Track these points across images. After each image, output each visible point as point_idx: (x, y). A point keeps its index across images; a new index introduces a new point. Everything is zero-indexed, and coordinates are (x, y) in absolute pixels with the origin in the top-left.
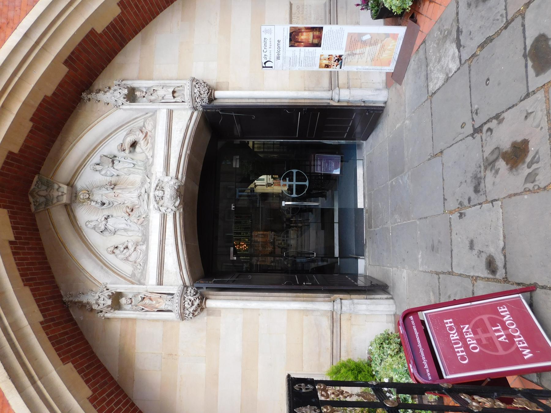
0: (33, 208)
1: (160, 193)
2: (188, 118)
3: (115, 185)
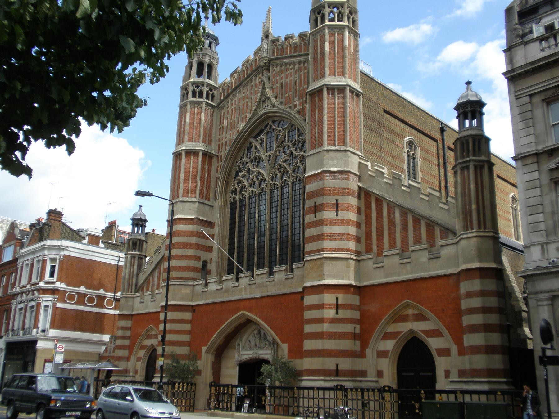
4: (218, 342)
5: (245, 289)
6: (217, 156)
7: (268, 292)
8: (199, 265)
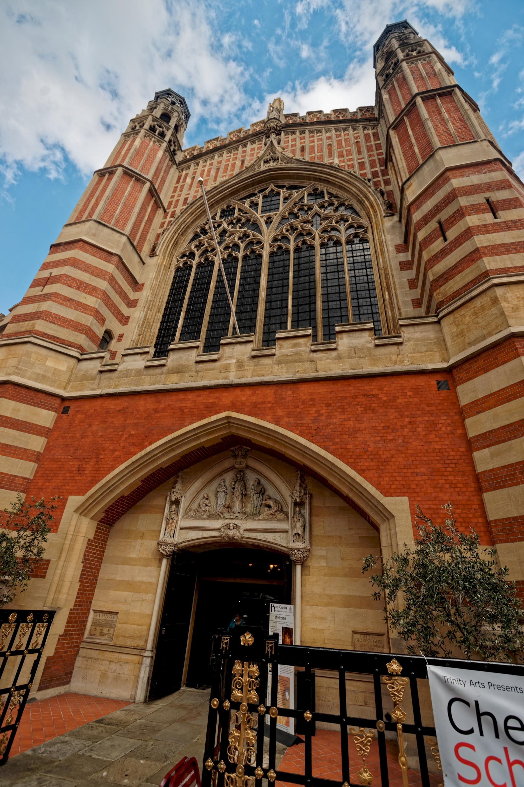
0: (232, 449)
1: (232, 528)
2: (283, 544)
3: (246, 495)
4: (122, 487)
5: (240, 365)
6: (165, 211)
7: (317, 371)
8: (100, 332)
